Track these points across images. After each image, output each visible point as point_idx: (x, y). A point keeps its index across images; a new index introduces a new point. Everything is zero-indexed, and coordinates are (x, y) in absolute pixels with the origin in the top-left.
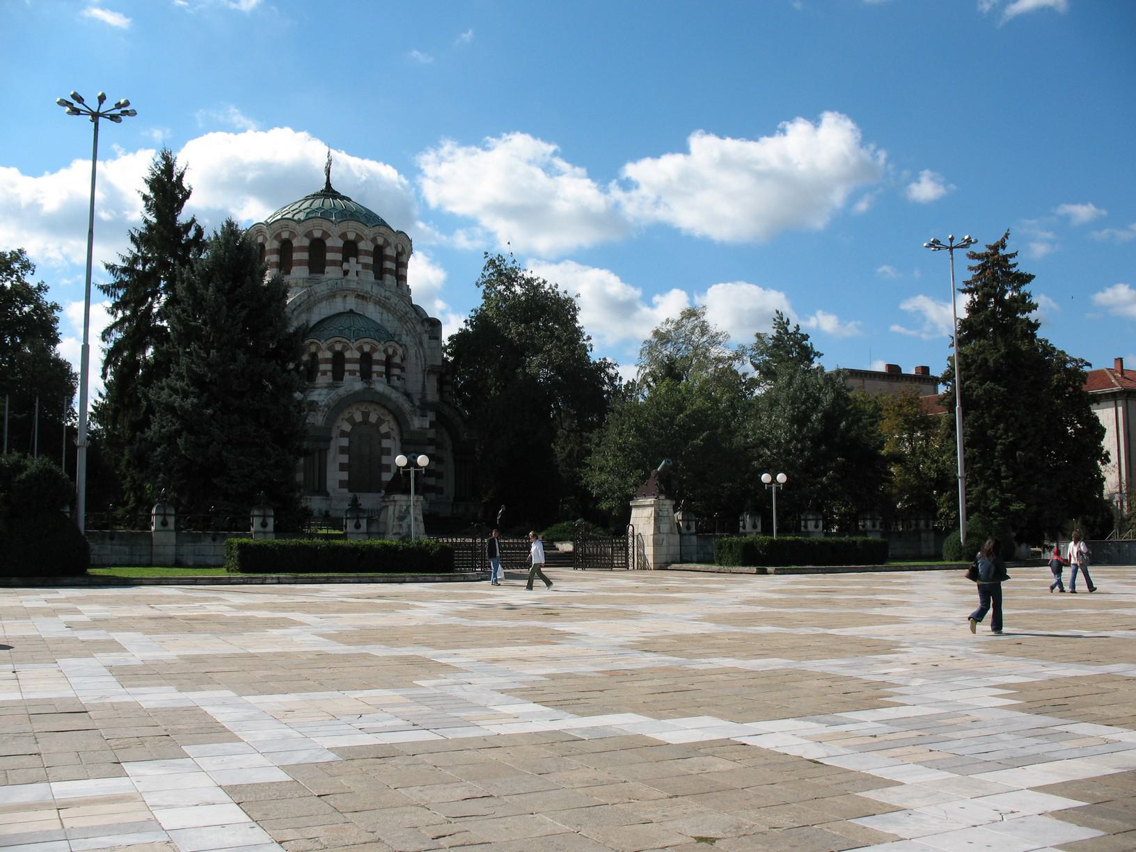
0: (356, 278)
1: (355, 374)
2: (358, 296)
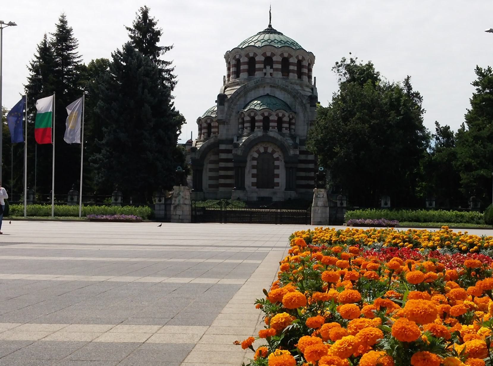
0: (270, 77)
1: (260, 128)
2: (271, 86)
